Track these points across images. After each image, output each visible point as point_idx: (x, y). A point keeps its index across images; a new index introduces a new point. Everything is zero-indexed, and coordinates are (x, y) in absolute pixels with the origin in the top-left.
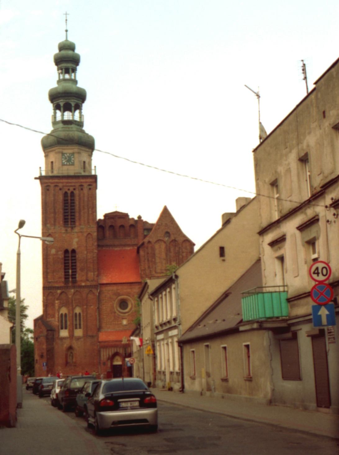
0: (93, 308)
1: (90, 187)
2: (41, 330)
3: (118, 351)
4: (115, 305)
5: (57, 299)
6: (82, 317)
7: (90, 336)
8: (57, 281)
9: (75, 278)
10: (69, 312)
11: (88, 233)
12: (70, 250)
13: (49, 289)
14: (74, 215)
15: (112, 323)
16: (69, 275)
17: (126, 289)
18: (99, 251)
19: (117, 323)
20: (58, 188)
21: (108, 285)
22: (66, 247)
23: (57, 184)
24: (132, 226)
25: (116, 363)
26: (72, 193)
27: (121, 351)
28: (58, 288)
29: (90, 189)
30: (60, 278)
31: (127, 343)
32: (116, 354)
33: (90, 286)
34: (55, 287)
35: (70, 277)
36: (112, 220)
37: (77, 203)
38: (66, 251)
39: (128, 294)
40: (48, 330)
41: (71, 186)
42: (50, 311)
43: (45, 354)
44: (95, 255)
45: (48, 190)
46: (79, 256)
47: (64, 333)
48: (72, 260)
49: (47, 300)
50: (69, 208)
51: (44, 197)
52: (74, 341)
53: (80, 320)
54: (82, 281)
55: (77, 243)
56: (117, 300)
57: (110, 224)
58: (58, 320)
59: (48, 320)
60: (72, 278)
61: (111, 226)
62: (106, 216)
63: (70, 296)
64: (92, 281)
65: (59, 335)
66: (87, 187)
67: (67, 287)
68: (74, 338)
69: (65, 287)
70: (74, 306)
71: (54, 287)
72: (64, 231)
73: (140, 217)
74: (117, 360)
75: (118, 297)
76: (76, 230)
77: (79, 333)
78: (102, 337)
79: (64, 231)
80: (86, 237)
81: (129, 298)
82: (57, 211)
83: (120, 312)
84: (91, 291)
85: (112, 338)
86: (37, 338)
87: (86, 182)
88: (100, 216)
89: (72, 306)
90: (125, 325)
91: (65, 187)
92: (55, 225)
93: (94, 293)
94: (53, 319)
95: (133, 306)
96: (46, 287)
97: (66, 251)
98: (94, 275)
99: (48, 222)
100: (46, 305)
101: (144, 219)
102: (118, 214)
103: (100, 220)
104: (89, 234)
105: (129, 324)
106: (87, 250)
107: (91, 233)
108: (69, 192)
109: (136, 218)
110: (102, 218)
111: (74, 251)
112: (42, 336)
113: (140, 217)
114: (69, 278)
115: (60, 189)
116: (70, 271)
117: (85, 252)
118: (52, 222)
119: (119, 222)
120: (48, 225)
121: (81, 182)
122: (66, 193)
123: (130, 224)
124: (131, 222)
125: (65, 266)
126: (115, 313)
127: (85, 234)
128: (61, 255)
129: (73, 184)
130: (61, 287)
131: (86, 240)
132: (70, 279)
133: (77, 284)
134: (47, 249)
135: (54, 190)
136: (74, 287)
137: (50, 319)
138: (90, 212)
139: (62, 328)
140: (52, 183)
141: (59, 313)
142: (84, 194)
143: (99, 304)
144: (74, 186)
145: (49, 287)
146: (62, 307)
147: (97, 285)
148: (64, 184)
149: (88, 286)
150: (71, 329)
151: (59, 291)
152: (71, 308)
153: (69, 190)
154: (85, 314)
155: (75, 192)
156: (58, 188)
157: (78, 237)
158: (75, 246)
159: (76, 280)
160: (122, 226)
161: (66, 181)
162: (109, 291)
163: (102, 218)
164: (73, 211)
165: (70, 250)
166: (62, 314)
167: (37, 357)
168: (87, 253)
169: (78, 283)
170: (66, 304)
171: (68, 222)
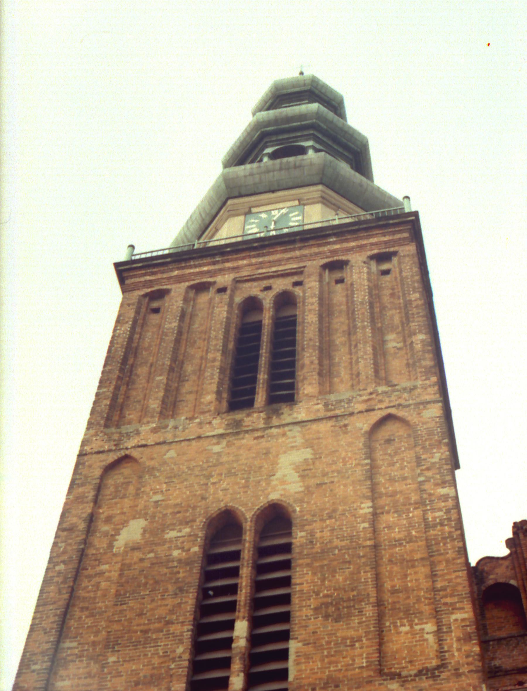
11: (377, 415)
79: (221, 431)
104: (389, 418)
107: (401, 413)
121: (334, 252)
129: (293, 266)
144: (299, 272)
153: (268, 288)
155: (298, 291)
168: (375, 515)
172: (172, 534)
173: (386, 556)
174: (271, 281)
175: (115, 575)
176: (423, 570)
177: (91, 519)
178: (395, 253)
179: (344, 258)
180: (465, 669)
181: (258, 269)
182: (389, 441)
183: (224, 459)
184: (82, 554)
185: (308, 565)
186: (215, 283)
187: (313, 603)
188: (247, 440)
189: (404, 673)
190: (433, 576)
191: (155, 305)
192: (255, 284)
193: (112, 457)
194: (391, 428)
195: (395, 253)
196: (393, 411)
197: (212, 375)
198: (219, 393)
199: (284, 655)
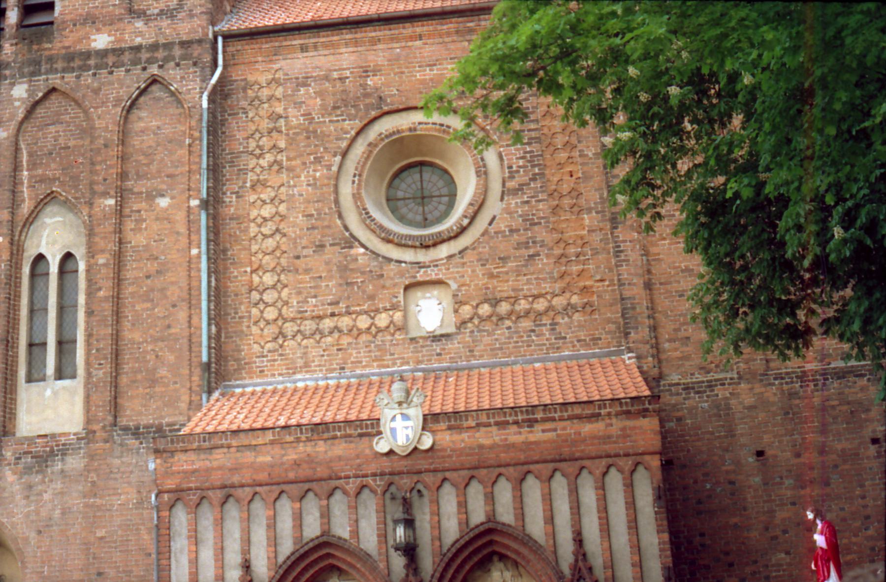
3: (342, 529)
7: (136, 432)
15: (328, 323)
19: (363, 322)
31: (427, 442)
33: (154, 47)
53: (65, 309)
56: (359, 149)
64: (168, 13)
70: (26, 208)
90: (436, 338)
95: (496, 187)
126: (352, 241)
143: (215, 171)
147: (200, 42)
149: (138, 49)
162: (304, 83)
180: (198, 10)
189: (148, 12)
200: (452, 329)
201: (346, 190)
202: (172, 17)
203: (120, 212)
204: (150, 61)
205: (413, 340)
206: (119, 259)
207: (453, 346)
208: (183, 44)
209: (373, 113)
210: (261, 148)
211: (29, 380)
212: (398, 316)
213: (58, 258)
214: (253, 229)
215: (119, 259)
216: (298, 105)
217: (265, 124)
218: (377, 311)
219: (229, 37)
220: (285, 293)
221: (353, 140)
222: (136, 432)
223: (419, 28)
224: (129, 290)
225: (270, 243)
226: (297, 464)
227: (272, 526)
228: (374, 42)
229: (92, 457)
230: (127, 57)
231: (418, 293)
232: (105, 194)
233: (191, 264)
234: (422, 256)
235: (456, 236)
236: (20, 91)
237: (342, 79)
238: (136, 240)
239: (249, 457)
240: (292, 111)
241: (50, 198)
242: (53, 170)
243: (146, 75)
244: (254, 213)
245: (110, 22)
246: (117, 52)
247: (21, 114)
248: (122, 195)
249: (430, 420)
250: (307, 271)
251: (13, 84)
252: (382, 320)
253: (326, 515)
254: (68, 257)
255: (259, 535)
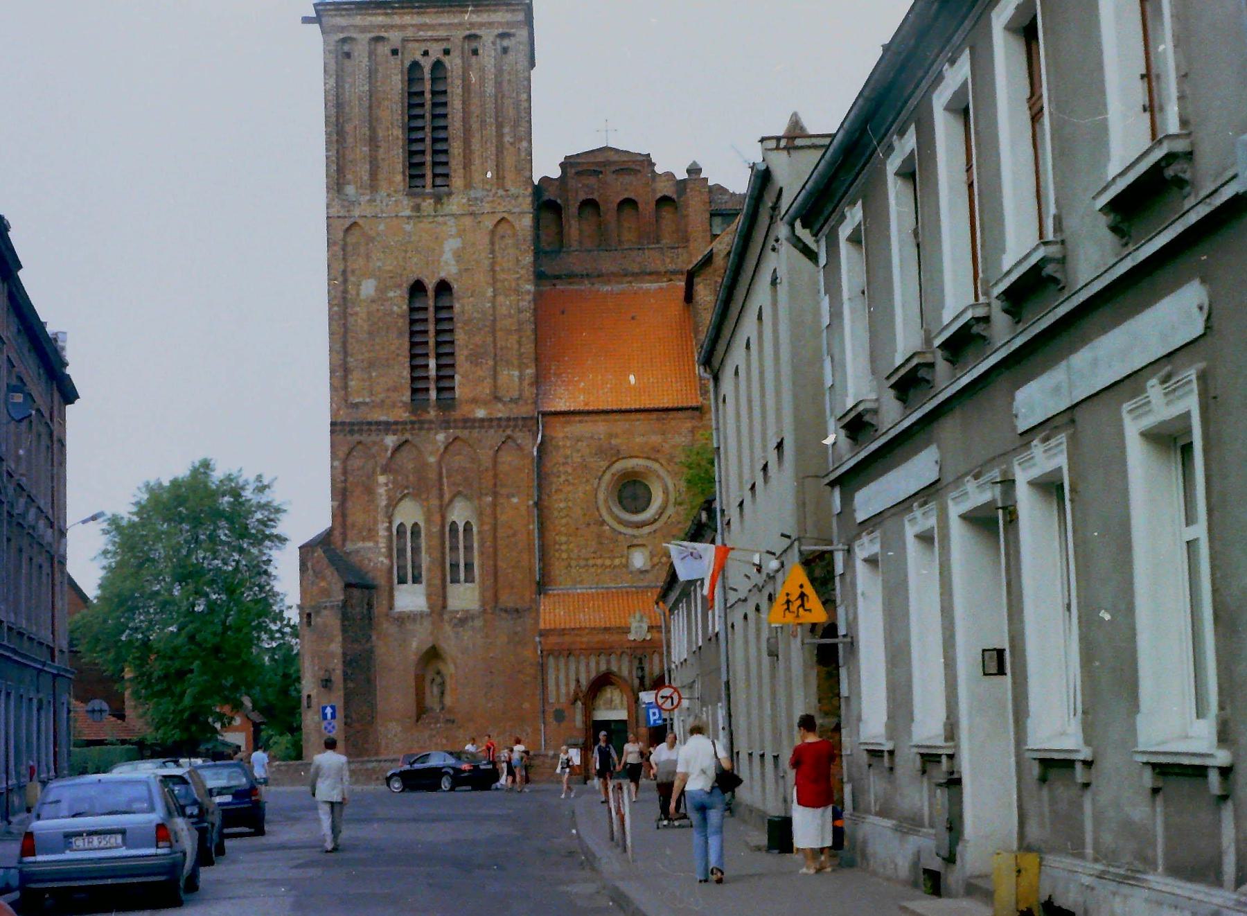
0: (517, 505)
1: (506, 43)
2: (323, 584)
3: (614, 668)
4: (601, 496)
5: (385, 470)
6: (476, 538)
7: (506, 611)
8: (383, 401)
9: (453, 388)
10: (428, 520)
11: (498, 217)
12: (430, 285)
13: (352, 432)
14: (446, 152)
15: (591, 562)
16: (427, 378)
17: (643, 434)
18: (538, 297)
19: (608, 562)
20: (384, 49)
21: (577, 418)
22: (417, 269)
23: (383, 34)
24: (664, 201)
25: (602, 715)
26: (438, 65)
27: (624, 668)
28: (387, 427)
29: (505, 50)
30: (395, 389)
31: (648, 638)
32: (603, 681)
33: (509, 419)
34: (378, 423)
35: (432, 386)
36: (592, 181)
37: (456, 104)
38: (417, 288)
39: (653, 453)
40: (348, 586)
41: (437, 40)
42: (357, 516)
43: (338, 675)
44: (526, 302)
45: (348, 55)
46: (463, 306)
47: (410, 599)
48: (438, 321)
49: (345, 472)
50: (427, 122)
51: (332, 82)
52: (448, 628)
53: (468, 549)
54: (474, 401)
55: (458, 256)
56: (607, 477)
57: (582, 196)
58: (390, 549)
59: (350, 547)
60: (439, 390)
61: (590, 205)
62: (568, 164)
63: (432, 460)
65: (391, 607)
66: (494, 43)
67: (418, 425)
68: (446, 617)
69: (412, 423)
70: (447, 497)
71: (370, 424)
72: (408, 213)
73: (694, 170)
74: (610, 705)
75: (614, 462)
76: (455, 204)
77: (464, 597)
78: (553, 613)
79: (408, 213)
80: (493, 232)
81: (656, 466)
82: (381, 134)
83: (621, 522)
84: (509, 437)
85: (590, 617)
86: (309, 615)
87: (491, 24)
88: (546, 166)
89: (441, 496)
90: (642, 572)
91: (410, 45)
92: (373, 187)
93: (520, 447)
94: (371, 544)
96: (343, 423)
97: (417, 288)
98: (521, 378)
99: (349, 177)
100: (342, 494)
101: (713, 177)
102: (615, 158)
103: (545, 180)
104: (503, 219)
105: (653, 566)
106: (495, 280)
107: (510, 218)
108: (427, 64)
109: (681, 175)
110: (556, 173)
111: (444, 287)
112: (325, 608)
113: (694, 170)
114: (427, 390)
115: (395, 52)
116: (432, 363)
117: (490, 292)
118: (366, 178)
119: (619, 188)
120: (350, 190)
121: (472, 25)
122: (415, 66)
123: (659, 195)
124: (665, 189)
125: (413, 345)
126: (603, 523)
127: (489, 223)
128: (398, 302)
129: (442, 33)
130: (396, 423)
131: (492, 243)
132: (433, 394)
133: (457, 414)
134: (345, 281)
135: (372, 54)
136: (446, 425)
137: (360, 544)
138: (507, 139)
139: (402, 581)
140: (363, 30)
141: (390, 523)
142: (482, 69)
144: (447, 39)
145: (353, 424)
146: (401, 499)
147: (532, 418)
148: (409, 33)
149: (500, 419)
150: (437, 582)
151: (390, 440)
152: (435, 502)
154: (486, 528)
155: (446, 60)
156: (384, 49)
157: (461, 233)
158: (448, 268)
159: (453, 399)
160: (629, 203)
161: (417, 20)
163: (556, 173)
164: (442, 134)
165: (430, 285)
166: (401, 524)
167: (308, 686)
168: (494, 297)
169: (462, 411)
170: (418, 488)
171: (423, 176)
172: (391, 294)
173: (499, 326)
174: (429, 44)
175: (364, 316)
176: (515, 337)
177: (344, 272)
178: (513, 35)
179: (478, 32)
180: (529, 402)
181: (420, 30)
182: (503, 237)
183: (413, 238)
184: (344, 298)
185: (463, 328)
186: (388, 39)
187: (466, 352)
188: (425, 225)
190: (519, 343)
191: (346, 48)
192: (416, 45)
193: (347, 223)
194: (504, 225)
195: (513, 35)
196: (505, 215)
197: (398, 154)
198: (404, 173)
199: (453, 377)
200: (648, 568)
201: (601, 496)
202: (516, 403)
203: (494, 505)
204: (507, 427)
205: (631, 572)
206: (495, 529)
207: (649, 576)
208: (524, 419)
209: (614, 459)
210: (559, 472)
211: (452, 582)
212: (624, 560)
213: (463, 523)
214: (556, 514)
215: (495, 529)
216: (578, 451)
217: (561, 460)
218: (614, 557)
219: (544, 414)
220: (571, 546)
221: (604, 472)
222: (506, 611)
223: (638, 416)
224: (499, 542)
225: (564, 521)
226: (598, 642)
227: (588, 665)
228: (616, 421)
229: (485, 621)
230: (495, 424)
231: (633, 549)
232: (486, 494)
233: (529, 533)
234: (635, 532)
235: (652, 523)
236: (441, 437)
237: (600, 439)
238: (503, 518)
239: (578, 639)
240: (574, 454)
241: (459, 493)
242: (458, 478)
243: (505, 434)
244: (556, 506)
245: (485, 403)
246: (491, 420)
247: (442, 450)
248: (495, 494)
249: (650, 628)
250: (582, 536)
251: (436, 434)
252: (617, 562)
253: (608, 662)
254: (467, 523)
255: (583, 669)
